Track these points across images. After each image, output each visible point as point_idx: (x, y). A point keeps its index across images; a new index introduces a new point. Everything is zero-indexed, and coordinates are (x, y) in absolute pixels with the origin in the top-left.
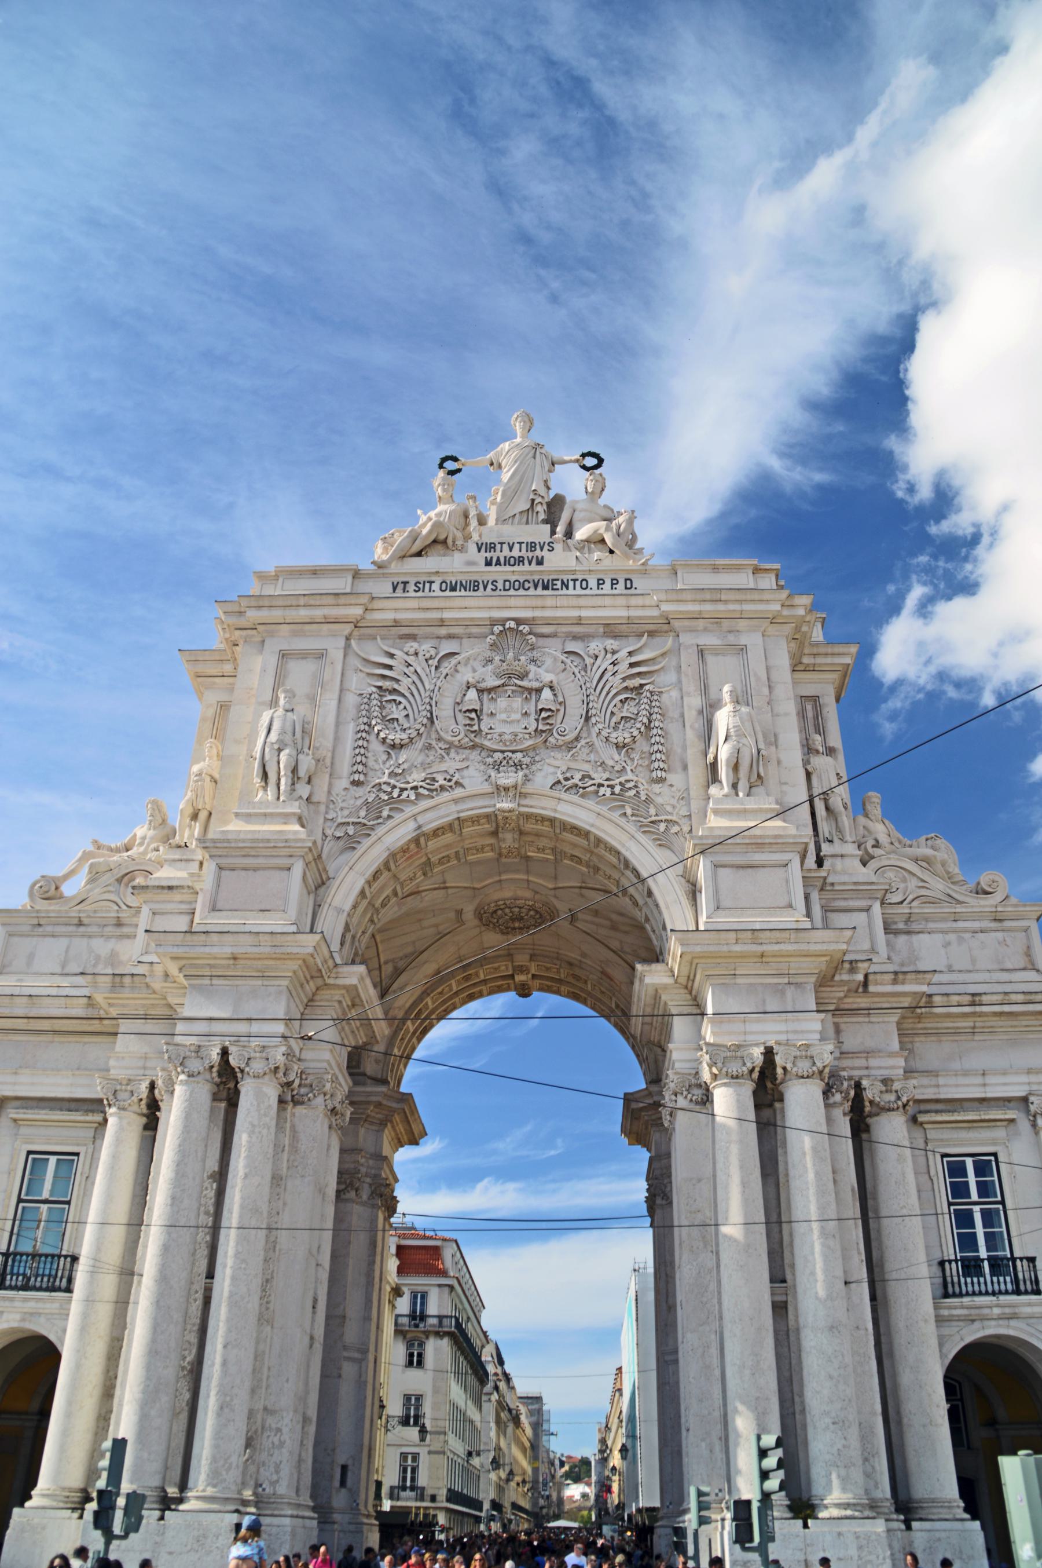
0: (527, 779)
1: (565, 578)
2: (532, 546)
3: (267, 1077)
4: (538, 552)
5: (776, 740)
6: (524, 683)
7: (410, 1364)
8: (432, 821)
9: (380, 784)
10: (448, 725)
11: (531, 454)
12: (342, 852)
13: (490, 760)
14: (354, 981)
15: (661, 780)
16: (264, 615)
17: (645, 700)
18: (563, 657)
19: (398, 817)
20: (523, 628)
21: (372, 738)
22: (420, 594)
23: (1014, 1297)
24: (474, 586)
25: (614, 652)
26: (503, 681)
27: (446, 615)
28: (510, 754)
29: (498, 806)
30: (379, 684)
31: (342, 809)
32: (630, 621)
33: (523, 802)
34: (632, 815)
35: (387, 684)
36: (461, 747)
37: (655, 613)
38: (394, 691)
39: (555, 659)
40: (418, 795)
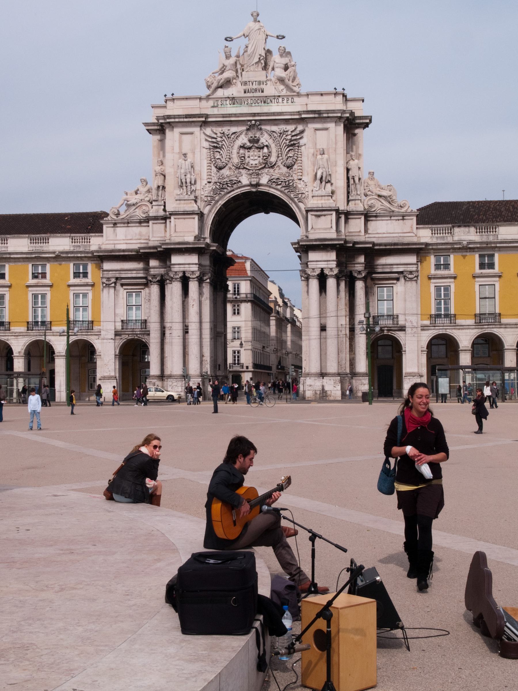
2: (260, 83)
3: (195, 279)
4: (262, 86)
7: (234, 313)
9: (216, 183)
10: (236, 160)
11: (258, 33)
13: (249, 172)
14: (215, 248)
15: (300, 179)
16: (172, 120)
17: (296, 150)
19: (223, 193)
20: (258, 123)
21: (212, 165)
22: (223, 106)
25: (287, 131)
26: (251, 145)
28: (254, 171)
29: (252, 190)
30: (213, 145)
31: (205, 191)
33: (259, 188)
34: (292, 191)
35: (215, 145)
36: (239, 168)
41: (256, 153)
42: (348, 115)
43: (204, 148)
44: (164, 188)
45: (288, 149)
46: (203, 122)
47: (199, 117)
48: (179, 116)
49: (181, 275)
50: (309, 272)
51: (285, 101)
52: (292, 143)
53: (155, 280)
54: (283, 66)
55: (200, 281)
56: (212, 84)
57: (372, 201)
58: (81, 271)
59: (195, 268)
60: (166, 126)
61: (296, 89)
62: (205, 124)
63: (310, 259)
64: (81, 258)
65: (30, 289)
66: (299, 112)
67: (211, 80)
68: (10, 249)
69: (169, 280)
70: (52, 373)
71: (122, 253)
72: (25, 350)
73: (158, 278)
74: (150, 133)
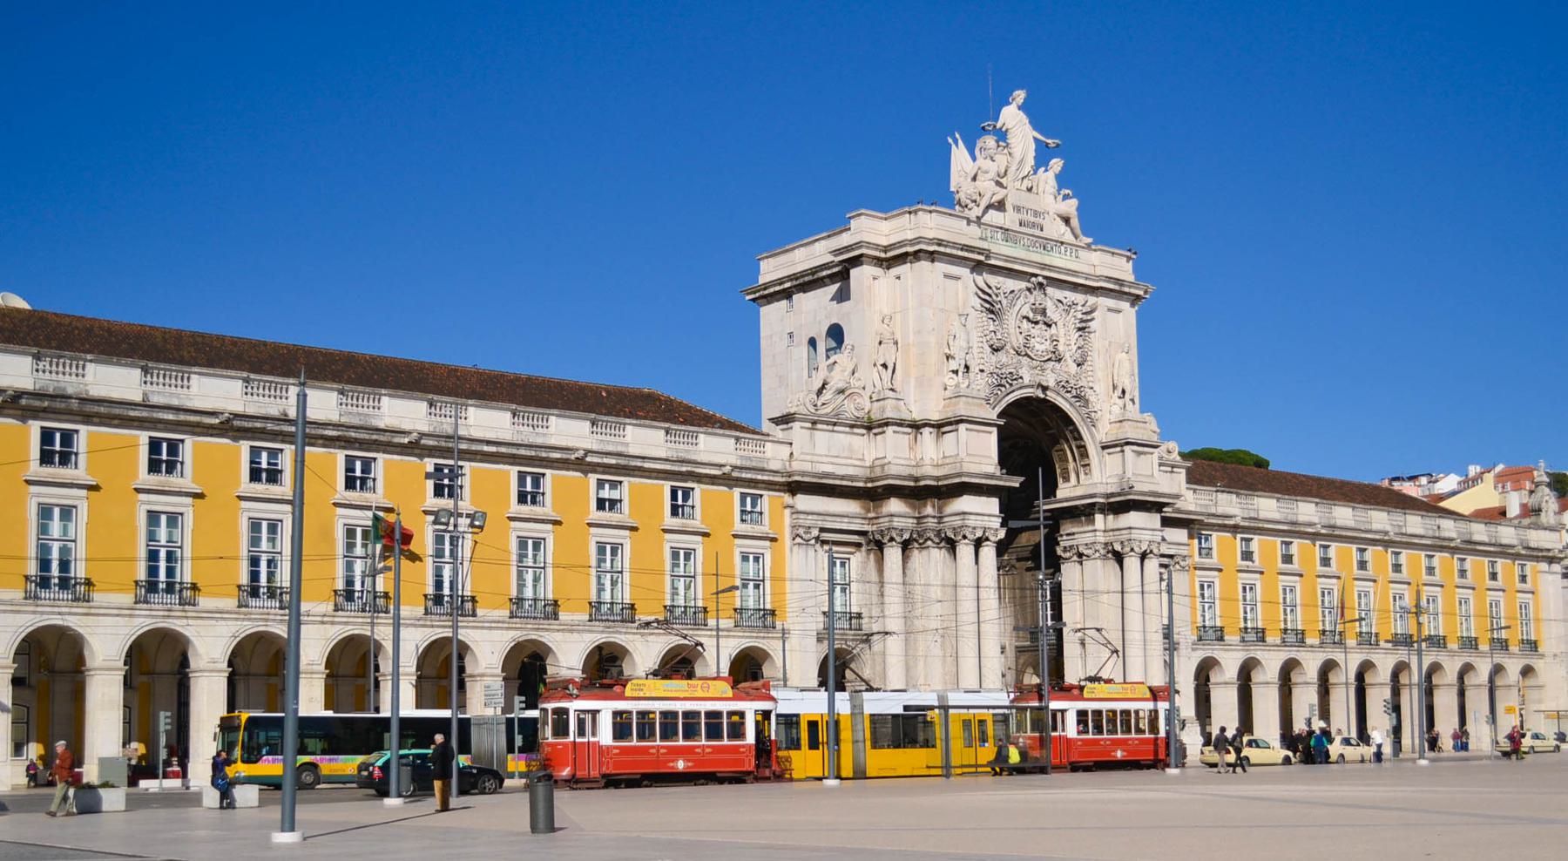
2: (1036, 213)
4: (1038, 220)
15: (1092, 388)
16: (942, 249)
18: (1057, 302)
36: (1019, 355)
40: (1008, 382)
43: (973, 307)
45: (1077, 335)
46: (979, 263)
47: (979, 253)
48: (954, 245)
49: (979, 534)
51: (1068, 253)
52: (1084, 325)
62: (978, 267)
69: (932, 540)
71: (838, 482)
73: (906, 536)
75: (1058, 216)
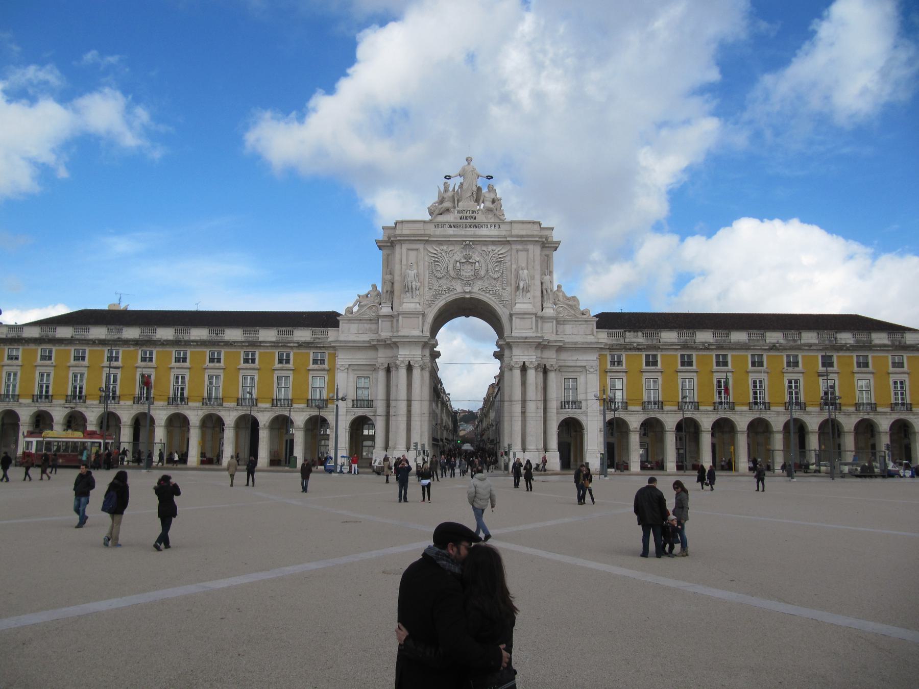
0: (472, 288)
1: (482, 224)
2: (472, 212)
5: (534, 278)
6: (470, 261)
8: (450, 299)
10: (452, 273)
12: (428, 308)
15: (505, 289)
23: (576, 410)
24: (456, 226)
27: (451, 239)
32: (499, 241)
35: (436, 259)
37: (505, 240)
38: (437, 261)
39: (479, 252)
41: (469, 267)
42: (544, 240)
44: (392, 292)
46: (427, 241)
47: (424, 237)
50: (512, 363)
53: (381, 367)
54: (491, 200)
55: (422, 369)
56: (434, 211)
57: (561, 309)
58: (319, 358)
59: (419, 358)
60: (396, 243)
61: (502, 217)
63: (513, 354)
64: (320, 347)
65: (276, 372)
66: (505, 235)
67: (433, 209)
68: (261, 339)
70: (292, 441)
72: (269, 423)
74: (380, 249)
75: (488, 210)
